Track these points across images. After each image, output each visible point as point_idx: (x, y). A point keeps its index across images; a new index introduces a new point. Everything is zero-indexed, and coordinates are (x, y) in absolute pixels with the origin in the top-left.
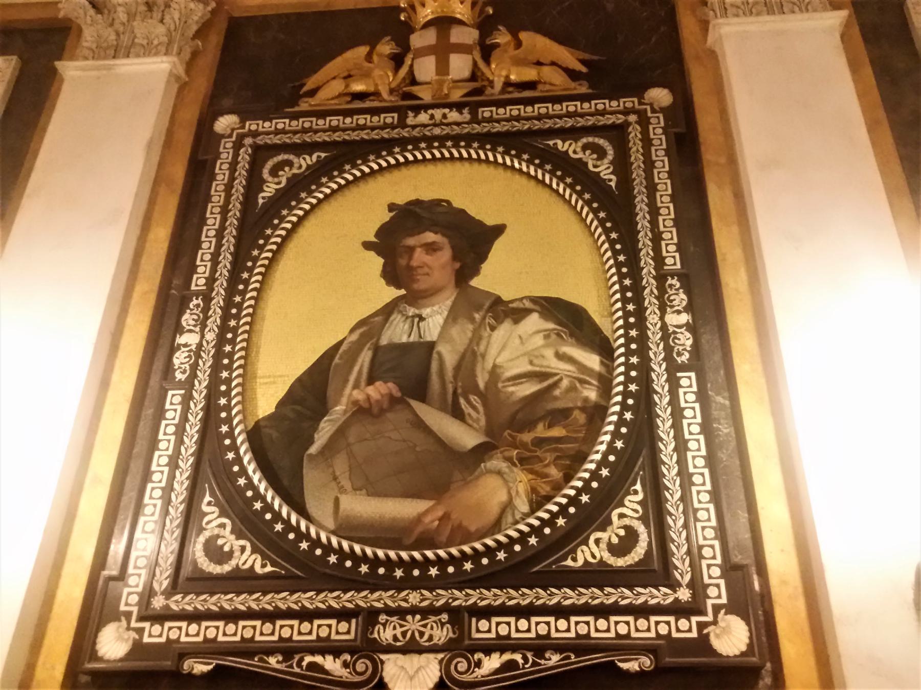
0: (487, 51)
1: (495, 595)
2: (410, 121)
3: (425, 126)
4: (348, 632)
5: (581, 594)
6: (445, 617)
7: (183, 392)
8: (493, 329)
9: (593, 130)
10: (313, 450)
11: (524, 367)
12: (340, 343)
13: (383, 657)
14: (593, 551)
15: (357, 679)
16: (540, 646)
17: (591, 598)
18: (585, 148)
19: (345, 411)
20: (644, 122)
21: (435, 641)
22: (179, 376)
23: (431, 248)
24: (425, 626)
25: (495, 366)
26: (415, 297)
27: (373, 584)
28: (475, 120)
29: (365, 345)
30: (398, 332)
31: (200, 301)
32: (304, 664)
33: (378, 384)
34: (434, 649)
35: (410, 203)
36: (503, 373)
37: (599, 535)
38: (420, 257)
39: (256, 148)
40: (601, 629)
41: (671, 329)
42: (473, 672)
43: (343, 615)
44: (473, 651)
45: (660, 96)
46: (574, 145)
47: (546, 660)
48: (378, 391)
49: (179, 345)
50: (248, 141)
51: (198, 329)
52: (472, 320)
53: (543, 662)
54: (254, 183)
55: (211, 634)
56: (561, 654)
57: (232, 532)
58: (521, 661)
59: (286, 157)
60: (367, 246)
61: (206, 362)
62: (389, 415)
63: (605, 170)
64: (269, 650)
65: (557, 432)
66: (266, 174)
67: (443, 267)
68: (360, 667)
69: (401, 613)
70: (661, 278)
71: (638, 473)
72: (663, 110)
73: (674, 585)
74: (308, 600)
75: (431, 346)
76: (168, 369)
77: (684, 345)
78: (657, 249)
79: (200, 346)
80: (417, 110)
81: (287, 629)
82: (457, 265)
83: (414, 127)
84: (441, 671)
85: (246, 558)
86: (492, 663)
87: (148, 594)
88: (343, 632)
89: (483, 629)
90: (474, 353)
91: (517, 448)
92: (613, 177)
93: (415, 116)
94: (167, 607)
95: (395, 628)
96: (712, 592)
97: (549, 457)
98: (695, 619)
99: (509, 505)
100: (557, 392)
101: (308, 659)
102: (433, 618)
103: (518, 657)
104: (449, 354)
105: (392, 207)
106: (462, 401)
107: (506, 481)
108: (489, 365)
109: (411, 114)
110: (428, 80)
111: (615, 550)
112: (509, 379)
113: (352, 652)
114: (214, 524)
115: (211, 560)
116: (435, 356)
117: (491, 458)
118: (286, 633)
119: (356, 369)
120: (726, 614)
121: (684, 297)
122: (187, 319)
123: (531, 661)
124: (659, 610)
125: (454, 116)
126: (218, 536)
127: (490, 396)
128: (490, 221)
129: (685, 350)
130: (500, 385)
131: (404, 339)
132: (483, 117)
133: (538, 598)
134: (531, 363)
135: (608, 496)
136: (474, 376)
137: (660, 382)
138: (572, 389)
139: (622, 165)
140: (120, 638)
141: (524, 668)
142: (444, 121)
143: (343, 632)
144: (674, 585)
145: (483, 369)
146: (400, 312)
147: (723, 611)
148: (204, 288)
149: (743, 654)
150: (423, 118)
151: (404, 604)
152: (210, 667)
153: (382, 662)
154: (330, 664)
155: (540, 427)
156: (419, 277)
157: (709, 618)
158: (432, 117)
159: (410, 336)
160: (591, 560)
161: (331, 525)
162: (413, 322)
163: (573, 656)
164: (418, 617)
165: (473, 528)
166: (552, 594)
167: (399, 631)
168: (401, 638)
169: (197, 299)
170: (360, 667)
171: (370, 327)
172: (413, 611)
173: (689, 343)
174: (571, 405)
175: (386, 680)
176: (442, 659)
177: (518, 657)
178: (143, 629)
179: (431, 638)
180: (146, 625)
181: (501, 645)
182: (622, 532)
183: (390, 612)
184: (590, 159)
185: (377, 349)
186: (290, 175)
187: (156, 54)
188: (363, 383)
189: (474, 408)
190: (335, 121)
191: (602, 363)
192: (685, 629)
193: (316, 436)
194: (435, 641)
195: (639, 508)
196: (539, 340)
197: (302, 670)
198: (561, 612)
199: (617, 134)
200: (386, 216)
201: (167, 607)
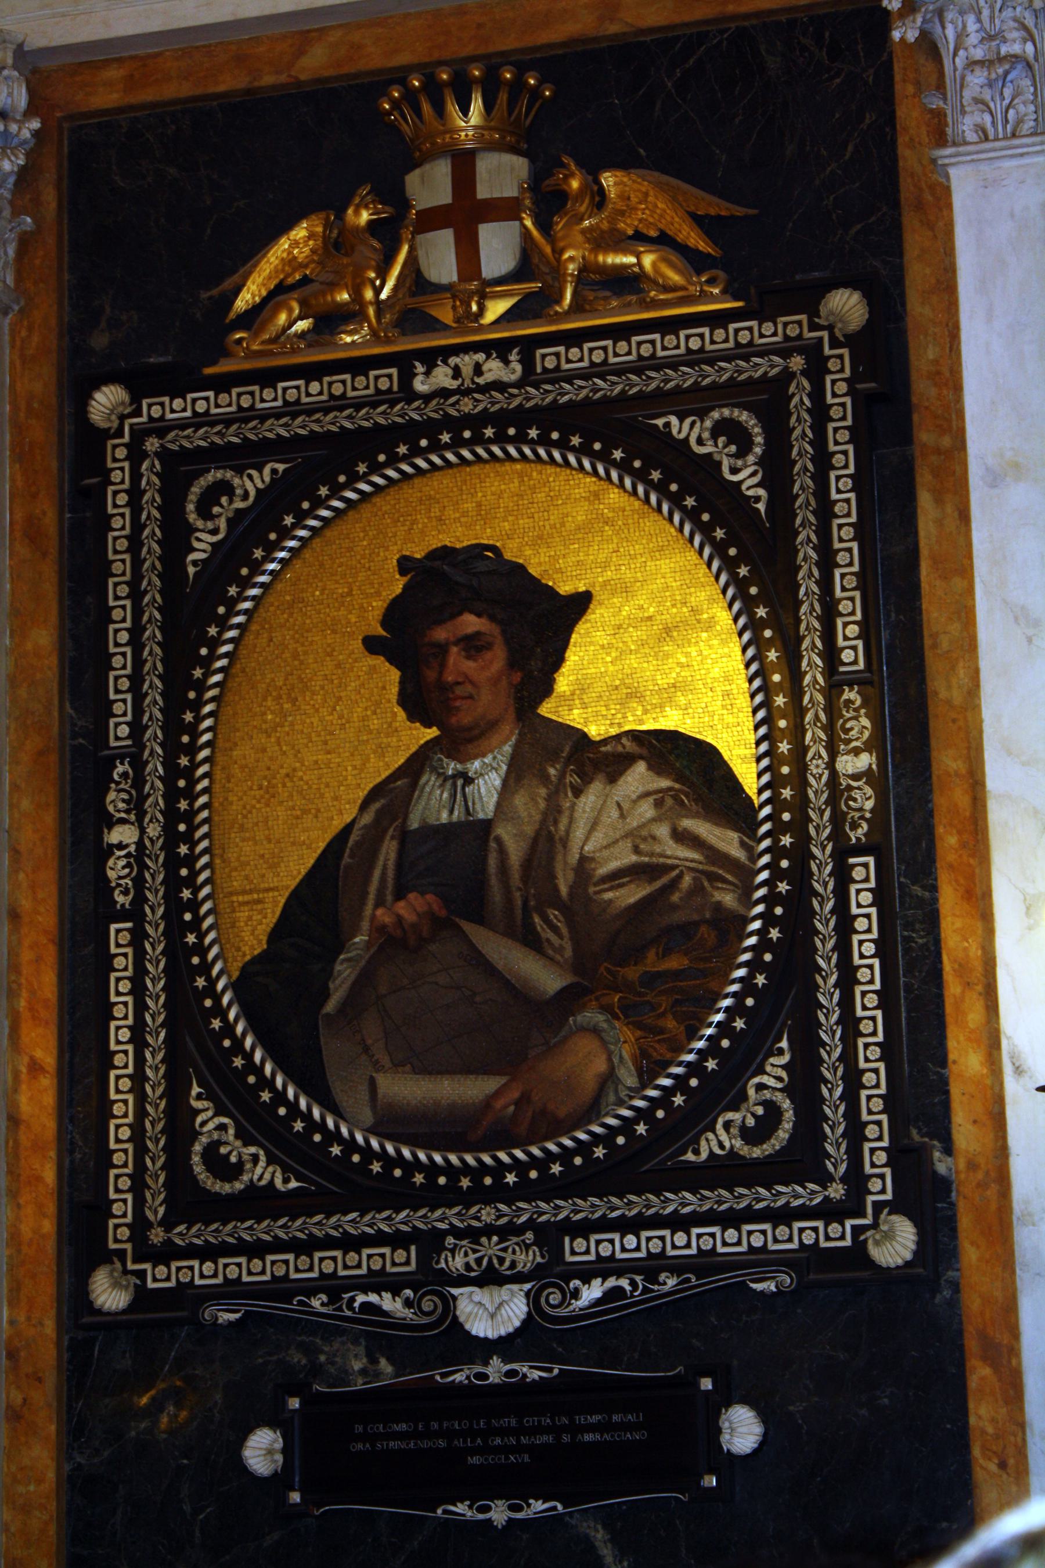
0: (548, 202)
1: (593, 1205)
2: (420, 385)
3: (444, 393)
4: (407, 1263)
5: (704, 1198)
6: (529, 1236)
7: (129, 925)
8: (578, 792)
9: (731, 392)
10: (330, 1007)
11: (624, 857)
12: (348, 829)
13: (455, 1291)
15: (425, 1320)
16: (651, 1267)
17: (717, 1202)
19: (368, 944)
21: (519, 1268)
23: (473, 645)
24: (505, 1250)
25: (583, 859)
26: (459, 742)
29: (385, 831)
30: (433, 805)
32: (356, 1305)
33: (412, 896)
34: (519, 1278)
35: (434, 555)
36: (594, 870)
37: (730, 1115)
38: (457, 662)
40: (726, 1241)
42: (569, 1304)
43: (397, 1240)
47: (660, 1284)
48: (411, 909)
49: (111, 846)
50: (152, 444)
51: (133, 817)
52: (545, 779)
53: (656, 1287)
55: (232, 1273)
57: (237, 1136)
58: (628, 1288)
59: (219, 475)
60: (372, 645)
61: (156, 876)
62: (433, 947)
64: (310, 1289)
65: (674, 963)
67: (495, 681)
68: (427, 1305)
69: (474, 1235)
71: (784, 1024)
73: (825, 1179)
74: (349, 1222)
75: (487, 825)
76: (104, 888)
77: (861, 809)
78: (829, 634)
79: (140, 844)
80: (431, 358)
81: (329, 1262)
82: (517, 677)
83: (427, 398)
84: (528, 1305)
86: (592, 1292)
87: (140, 1226)
88: (403, 1261)
89: (578, 1250)
90: (550, 838)
91: (617, 990)
92: (761, 492)
93: (427, 373)
94: (169, 1242)
95: (466, 1254)
97: (665, 1002)
99: (609, 1078)
100: (675, 898)
101: (361, 1298)
102: (515, 1239)
103: (624, 1283)
104: (513, 841)
105: (405, 564)
106: (537, 920)
107: (604, 1043)
108: (574, 858)
109: (420, 368)
110: (445, 280)
111: (749, 1136)
112: (605, 879)
114: (211, 1126)
115: (215, 1177)
116: (493, 845)
117: (583, 1008)
118: (328, 1267)
119: (377, 874)
120: (890, 1213)
121: (865, 722)
122: (115, 801)
123: (641, 1287)
124: (805, 1213)
125: (494, 369)
126: (219, 1143)
127: (579, 909)
128: (565, 588)
129: (862, 818)
130: (592, 890)
131: (444, 817)
132: (545, 370)
133: (648, 1207)
134: (636, 850)
135: (742, 1057)
136: (553, 877)
138: (697, 889)
140: (116, 1285)
141: (632, 1296)
142: (481, 381)
143: (403, 1261)
145: (566, 863)
146: (434, 770)
148: (129, 742)
149: (908, 1264)
150: (442, 377)
151: (475, 1223)
152: (237, 1316)
153: (455, 1298)
154: (388, 1303)
155: (651, 955)
156: (458, 703)
158: (457, 373)
159: (451, 812)
160: (718, 1151)
161: (367, 1117)
162: (455, 785)
165: (562, 1112)
166: (667, 1200)
167: (472, 1257)
168: (475, 1267)
169: (122, 763)
170: (427, 1305)
171: (392, 795)
172: (489, 1230)
174: (696, 917)
175: (462, 1319)
176: (530, 1290)
177: (624, 1283)
179: (513, 1265)
180: (147, 1266)
181: (605, 1267)
182: (760, 1111)
183: (458, 1233)
185: (404, 836)
186: (231, 515)
188: (389, 898)
189: (555, 929)
191: (743, 844)
192: (838, 1235)
193: (331, 986)
194: (519, 1268)
195: (784, 1075)
196: (647, 810)
197: (355, 1312)
198: (679, 1223)
200: (398, 585)
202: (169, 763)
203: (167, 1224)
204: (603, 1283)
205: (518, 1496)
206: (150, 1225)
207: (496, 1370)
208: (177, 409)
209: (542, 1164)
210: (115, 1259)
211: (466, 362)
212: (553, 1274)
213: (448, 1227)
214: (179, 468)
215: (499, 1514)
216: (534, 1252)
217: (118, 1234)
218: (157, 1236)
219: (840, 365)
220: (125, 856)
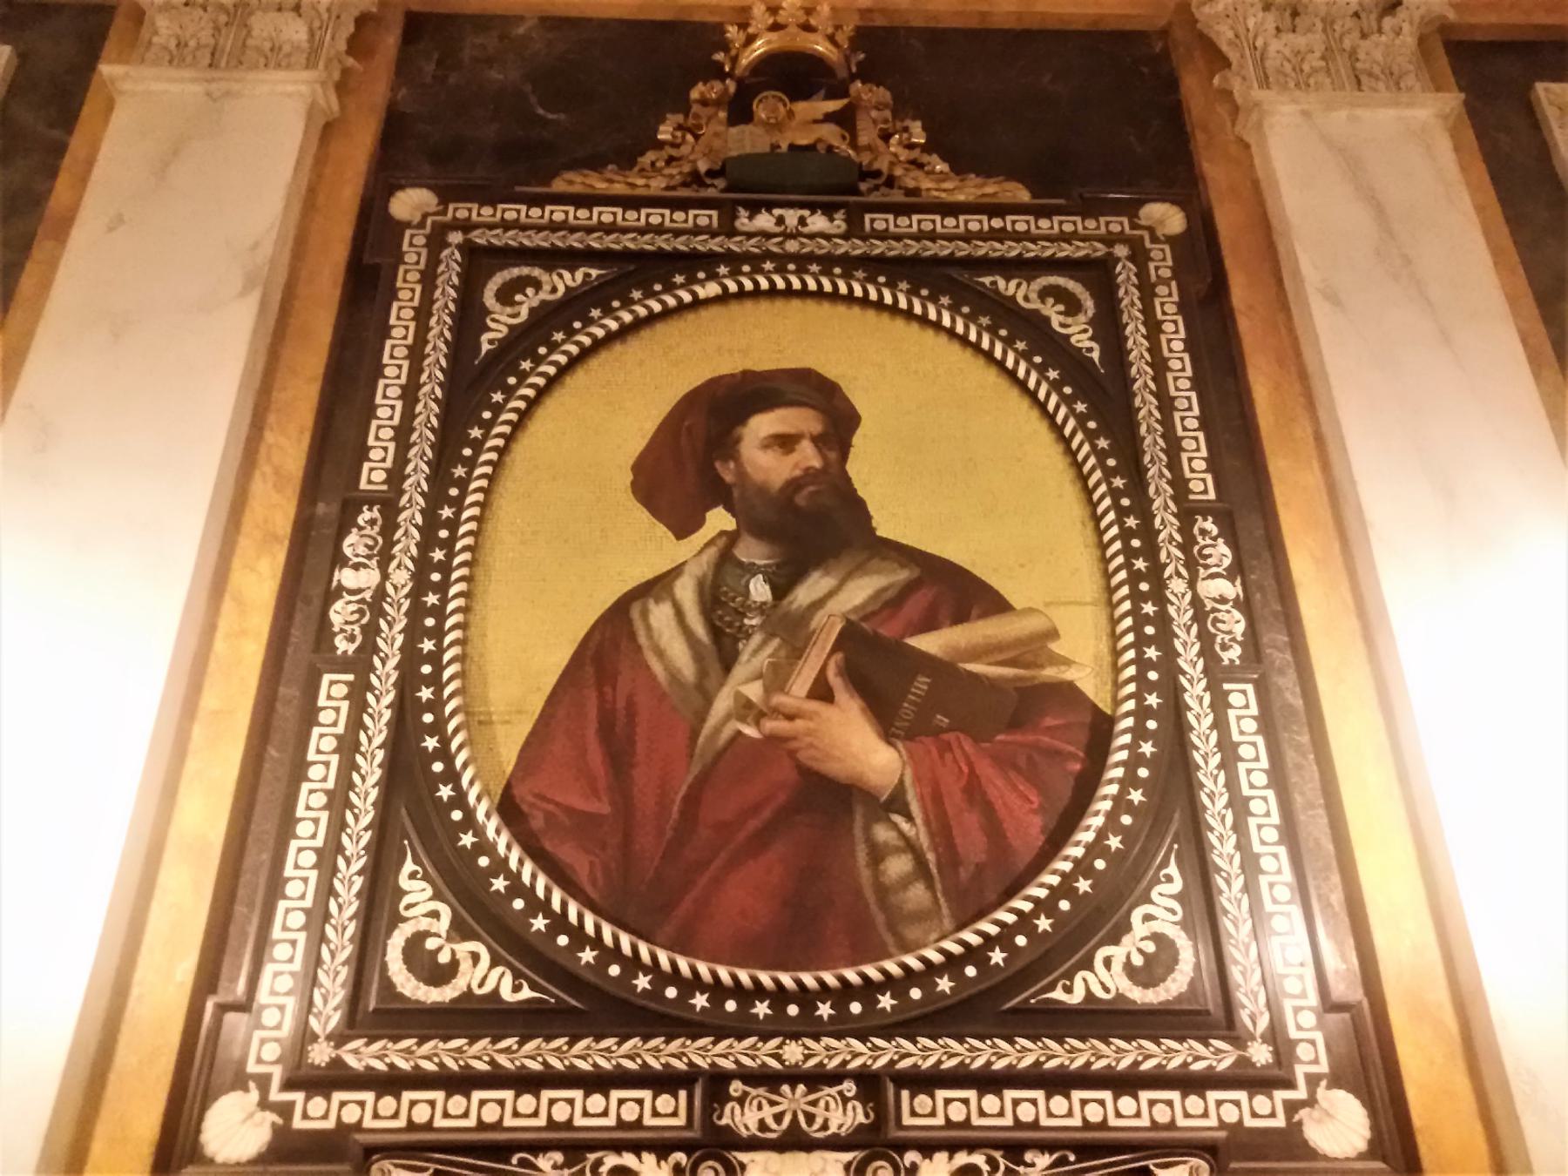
2: (743, 222)
3: (768, 235)
13: (744, 1157)
14: (1105, 976)
18: (1044, 294)
20: (1139, 256)
22: (342, 645)
24: (814, 1103)
31: (376, 514)
34: (835, 1144)
39: (468, 249)
41: (1209, 605)
44: (902, 1147)
45: (1167, 217)
46: (1024, 285)
51: (374, 562)
56: (1051, 1154)
58: (985, 1168)
63: (1080, 335)
66: (489, 299)
69: (769, 1080)
71: (1170, 849)
72: (1170, 240)
76: (324, 630)
77: (1230, 632)
81: (565, 1105)
83: (750, 235)
85: (482, 973)
93: (751, 218)
94: (337, 1062)
95: (760, 1107)
96: (1303, 1051)
98: (1280, 1095)
101: (611, 1160)
102: (827, 1090)
103: (979, 1159)
109: (743, 213)
113: (687, 1147)
115: (419, 978)
120: (1329, 1087)
121: (1226, 550)
122: (353, 544)
123: (1002, 1168)
125: (818, 222)
137: (1196, 694)
139: (1109, 327)
142: (805, 230)
144: (1237, 1038)
147: (1324, 1083)
148: (385, 487)
150: (764, 221)
153: (743, 1167)
157: (1300, 1093)
158: (780, 221)
163: (1072, 1158)
164: (801, 1088)
167: (768, 1113)
168: (774, 1126)
169: (370, 509)
172: (793, 1077)
173: (1239, 629)
178: (291, 1105)
179: (825, 1127)
180: (298, 1097)
182: (1150, 947)
184: (1054, 313)
186: (535, 303)
187: (289, 67)
190: (606, 215)
192: (1260, 1112)
199: (1098, 273)
201: (337, 1062)
202: (430, 513)
203: (339, 1039)
204: (951, 1158)
206: (315, 1038)
209: (869, 990)
210: (252, 1085)
213: (734, 1066)
216: (854, 1108)
219: (1162, 262)
220: (358, 602)
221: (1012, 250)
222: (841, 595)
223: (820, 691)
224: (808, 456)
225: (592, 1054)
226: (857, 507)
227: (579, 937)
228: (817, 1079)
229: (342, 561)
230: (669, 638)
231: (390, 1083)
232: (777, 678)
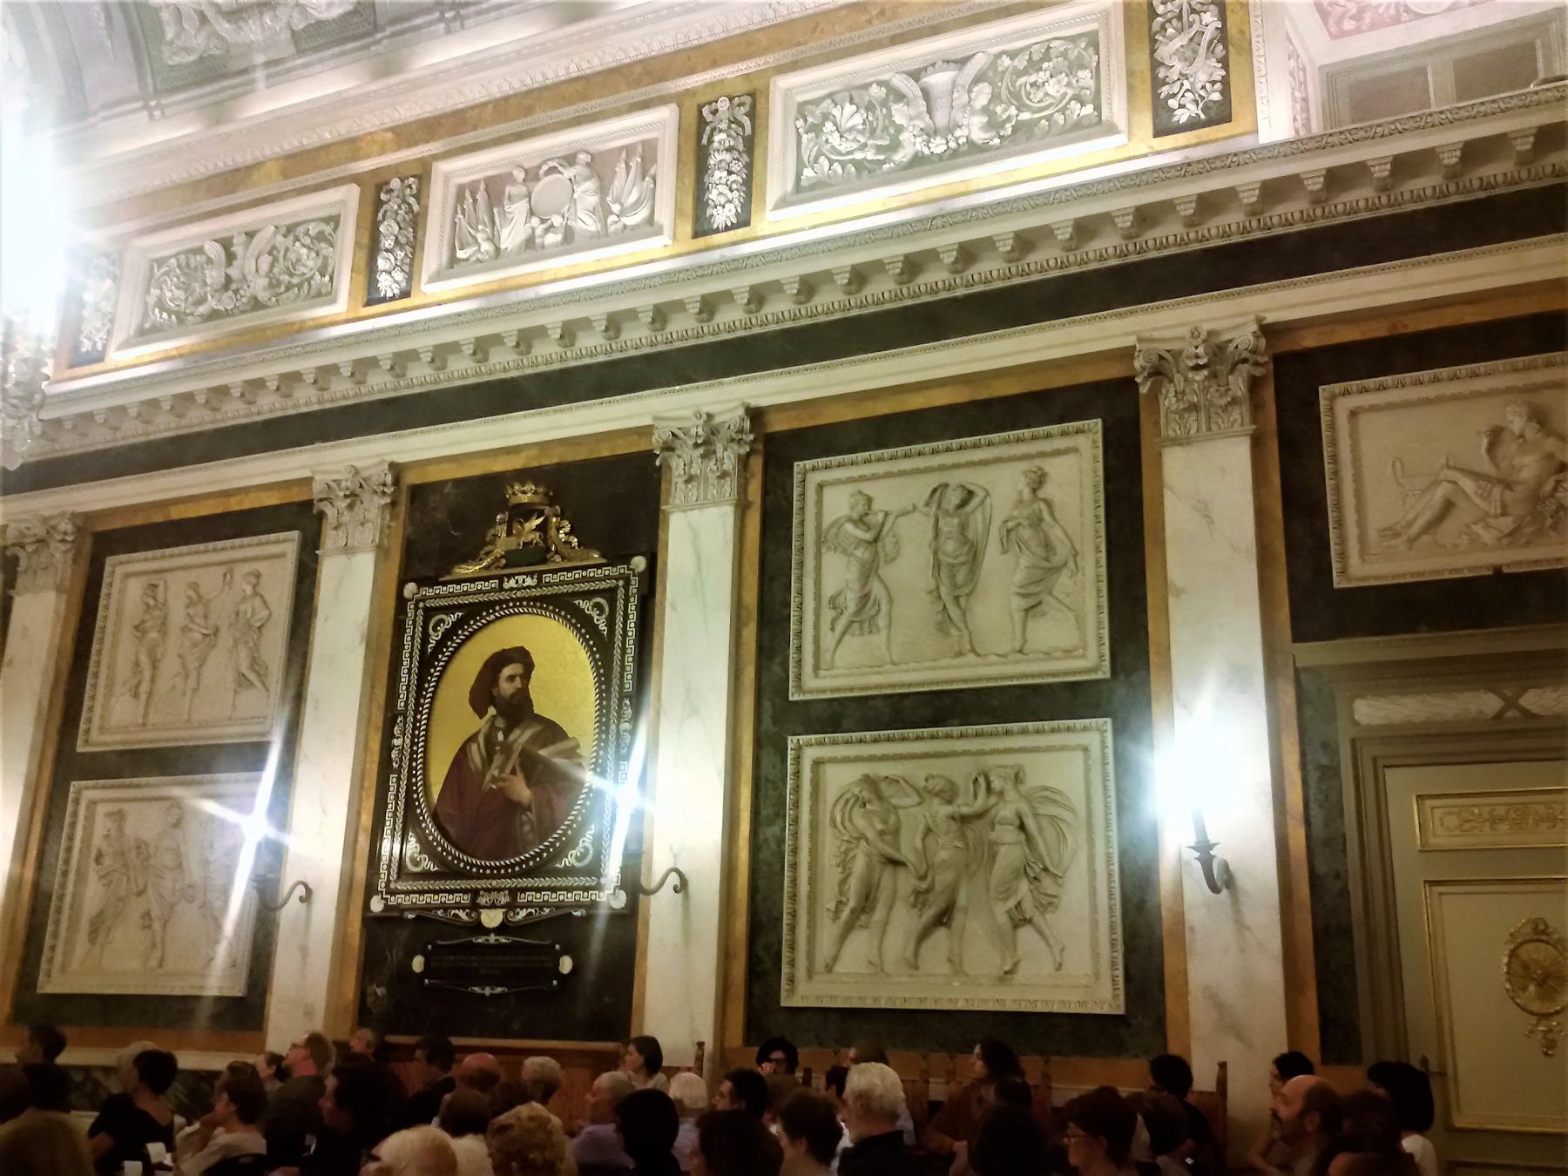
2: (506, 585)
3: (512, 589)
27: (479, 877)
28: (540, 584)
39: (426, 609)
43: (465, 891)
54: (425, 638)
69: (488, 890)
70: (620, 700)
76: (390, 761)
80: (510, 576)
87: (388, 882)
89: (522, 898)
122: (397, 730)
125: (529, 581)
143: (465, 899)
150: (512, 583)
172: (494, 889)
181: (529, 905)
190: (465, 587)
205: (493, 985)
207: (492, 938)
208: (429, 592)
209: (512, 866)
211: (520, 578)
212: (511, 906)
214: (429, 612)
215: (487, 991)
217: (382, 886)
218: (392, 886)
221: (585, 587)
222: (522, 737)
223: (513, 772)
224: (518, 683)
225: (450, 885)
226: (528, 702)
227: (449, 853)
228: (499, 890)
229: (393, 736)
230: (476, 754)
231: (407, 893)
232: (502, 769)
